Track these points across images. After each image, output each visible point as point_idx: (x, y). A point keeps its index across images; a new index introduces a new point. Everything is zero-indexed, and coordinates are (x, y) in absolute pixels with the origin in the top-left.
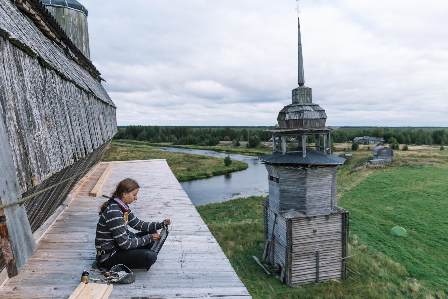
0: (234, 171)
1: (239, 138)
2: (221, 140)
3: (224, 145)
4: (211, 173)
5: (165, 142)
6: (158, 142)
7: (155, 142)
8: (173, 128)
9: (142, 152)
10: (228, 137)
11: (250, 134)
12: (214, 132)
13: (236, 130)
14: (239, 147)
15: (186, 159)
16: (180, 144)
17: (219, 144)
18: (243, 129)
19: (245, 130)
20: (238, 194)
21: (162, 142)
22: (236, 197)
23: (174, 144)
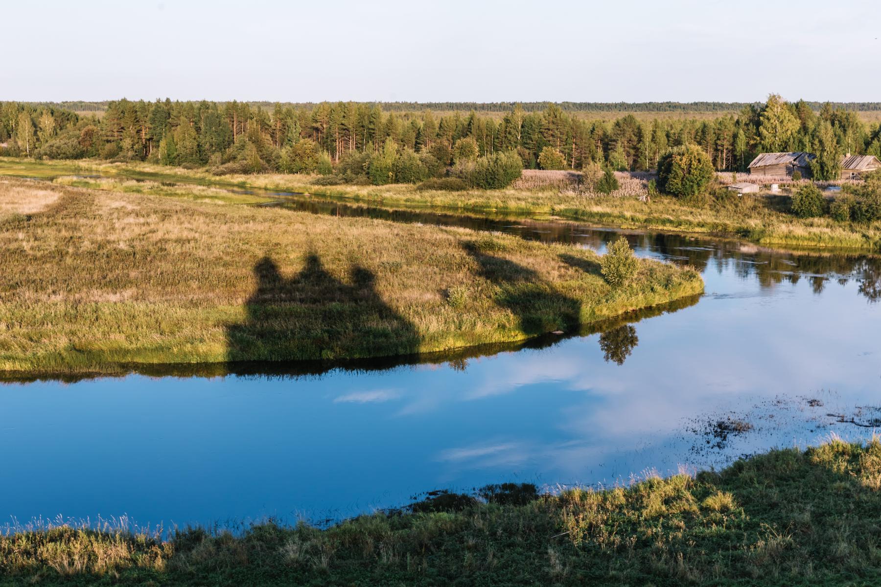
0: (650, 311)
1: (606, 158)
2: (527, 167)
3: (543, 189)
4: (559, 321)
5: (278, 169)
6: (246, 171)
7: (233, 171)
8: (310, 114)
9: (207, 215)
10: (557, 152)
11: (653, 140)
12: (489, 127)
13: (586, 120)
14: (615, 193)
15: (414, 251)
16: (347, 181)
17: (519, 183)
18: (621, 115)
19: (629, 121)
20: (739, 429)
21: (261, 170)
22: (741, 447)
23: (317, 183)
